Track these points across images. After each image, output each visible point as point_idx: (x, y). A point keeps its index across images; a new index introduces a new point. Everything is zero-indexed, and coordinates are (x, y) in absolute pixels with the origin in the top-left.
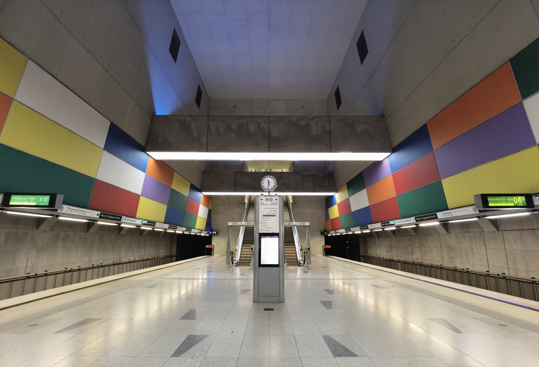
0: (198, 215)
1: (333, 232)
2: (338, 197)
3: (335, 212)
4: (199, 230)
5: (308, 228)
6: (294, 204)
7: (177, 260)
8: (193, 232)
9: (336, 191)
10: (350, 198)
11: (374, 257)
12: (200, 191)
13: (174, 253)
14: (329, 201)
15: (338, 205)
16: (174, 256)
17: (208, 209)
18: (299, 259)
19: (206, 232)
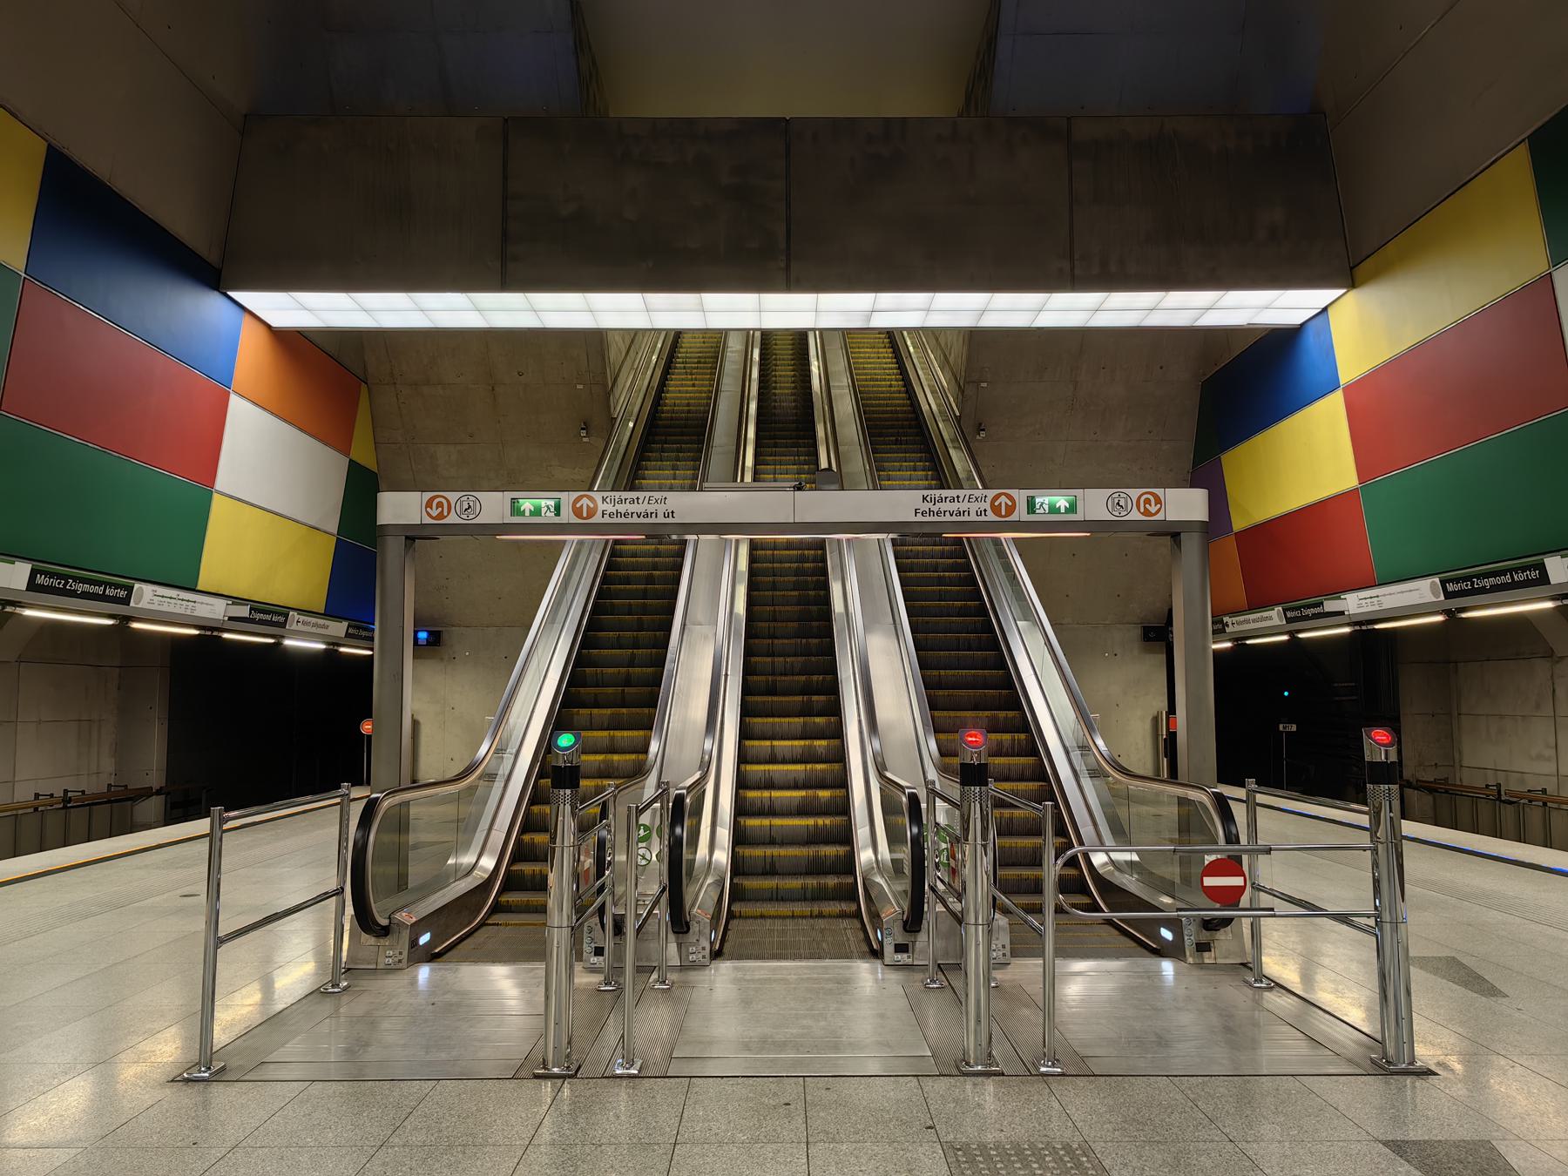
0: (220, 484)
1: (1275, 616)
2: (1361, 328)
3: (1310, 459)
4: (237, 600)
5: (1191, 544)
6: (971, 427)
7: (169, 820)
8: (160, 610)
9: (1352, 284)
10: (1556, 275)
11: (1544, 801)
12: (216, 278)
13: (151, 765)
14: (1251, 383)
15: (1350, 391)
16: (147, 793)
17: (343, 462)
18: (1098, 859)
19: (339, 628)
